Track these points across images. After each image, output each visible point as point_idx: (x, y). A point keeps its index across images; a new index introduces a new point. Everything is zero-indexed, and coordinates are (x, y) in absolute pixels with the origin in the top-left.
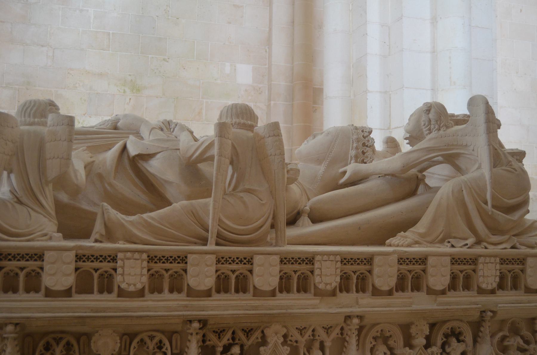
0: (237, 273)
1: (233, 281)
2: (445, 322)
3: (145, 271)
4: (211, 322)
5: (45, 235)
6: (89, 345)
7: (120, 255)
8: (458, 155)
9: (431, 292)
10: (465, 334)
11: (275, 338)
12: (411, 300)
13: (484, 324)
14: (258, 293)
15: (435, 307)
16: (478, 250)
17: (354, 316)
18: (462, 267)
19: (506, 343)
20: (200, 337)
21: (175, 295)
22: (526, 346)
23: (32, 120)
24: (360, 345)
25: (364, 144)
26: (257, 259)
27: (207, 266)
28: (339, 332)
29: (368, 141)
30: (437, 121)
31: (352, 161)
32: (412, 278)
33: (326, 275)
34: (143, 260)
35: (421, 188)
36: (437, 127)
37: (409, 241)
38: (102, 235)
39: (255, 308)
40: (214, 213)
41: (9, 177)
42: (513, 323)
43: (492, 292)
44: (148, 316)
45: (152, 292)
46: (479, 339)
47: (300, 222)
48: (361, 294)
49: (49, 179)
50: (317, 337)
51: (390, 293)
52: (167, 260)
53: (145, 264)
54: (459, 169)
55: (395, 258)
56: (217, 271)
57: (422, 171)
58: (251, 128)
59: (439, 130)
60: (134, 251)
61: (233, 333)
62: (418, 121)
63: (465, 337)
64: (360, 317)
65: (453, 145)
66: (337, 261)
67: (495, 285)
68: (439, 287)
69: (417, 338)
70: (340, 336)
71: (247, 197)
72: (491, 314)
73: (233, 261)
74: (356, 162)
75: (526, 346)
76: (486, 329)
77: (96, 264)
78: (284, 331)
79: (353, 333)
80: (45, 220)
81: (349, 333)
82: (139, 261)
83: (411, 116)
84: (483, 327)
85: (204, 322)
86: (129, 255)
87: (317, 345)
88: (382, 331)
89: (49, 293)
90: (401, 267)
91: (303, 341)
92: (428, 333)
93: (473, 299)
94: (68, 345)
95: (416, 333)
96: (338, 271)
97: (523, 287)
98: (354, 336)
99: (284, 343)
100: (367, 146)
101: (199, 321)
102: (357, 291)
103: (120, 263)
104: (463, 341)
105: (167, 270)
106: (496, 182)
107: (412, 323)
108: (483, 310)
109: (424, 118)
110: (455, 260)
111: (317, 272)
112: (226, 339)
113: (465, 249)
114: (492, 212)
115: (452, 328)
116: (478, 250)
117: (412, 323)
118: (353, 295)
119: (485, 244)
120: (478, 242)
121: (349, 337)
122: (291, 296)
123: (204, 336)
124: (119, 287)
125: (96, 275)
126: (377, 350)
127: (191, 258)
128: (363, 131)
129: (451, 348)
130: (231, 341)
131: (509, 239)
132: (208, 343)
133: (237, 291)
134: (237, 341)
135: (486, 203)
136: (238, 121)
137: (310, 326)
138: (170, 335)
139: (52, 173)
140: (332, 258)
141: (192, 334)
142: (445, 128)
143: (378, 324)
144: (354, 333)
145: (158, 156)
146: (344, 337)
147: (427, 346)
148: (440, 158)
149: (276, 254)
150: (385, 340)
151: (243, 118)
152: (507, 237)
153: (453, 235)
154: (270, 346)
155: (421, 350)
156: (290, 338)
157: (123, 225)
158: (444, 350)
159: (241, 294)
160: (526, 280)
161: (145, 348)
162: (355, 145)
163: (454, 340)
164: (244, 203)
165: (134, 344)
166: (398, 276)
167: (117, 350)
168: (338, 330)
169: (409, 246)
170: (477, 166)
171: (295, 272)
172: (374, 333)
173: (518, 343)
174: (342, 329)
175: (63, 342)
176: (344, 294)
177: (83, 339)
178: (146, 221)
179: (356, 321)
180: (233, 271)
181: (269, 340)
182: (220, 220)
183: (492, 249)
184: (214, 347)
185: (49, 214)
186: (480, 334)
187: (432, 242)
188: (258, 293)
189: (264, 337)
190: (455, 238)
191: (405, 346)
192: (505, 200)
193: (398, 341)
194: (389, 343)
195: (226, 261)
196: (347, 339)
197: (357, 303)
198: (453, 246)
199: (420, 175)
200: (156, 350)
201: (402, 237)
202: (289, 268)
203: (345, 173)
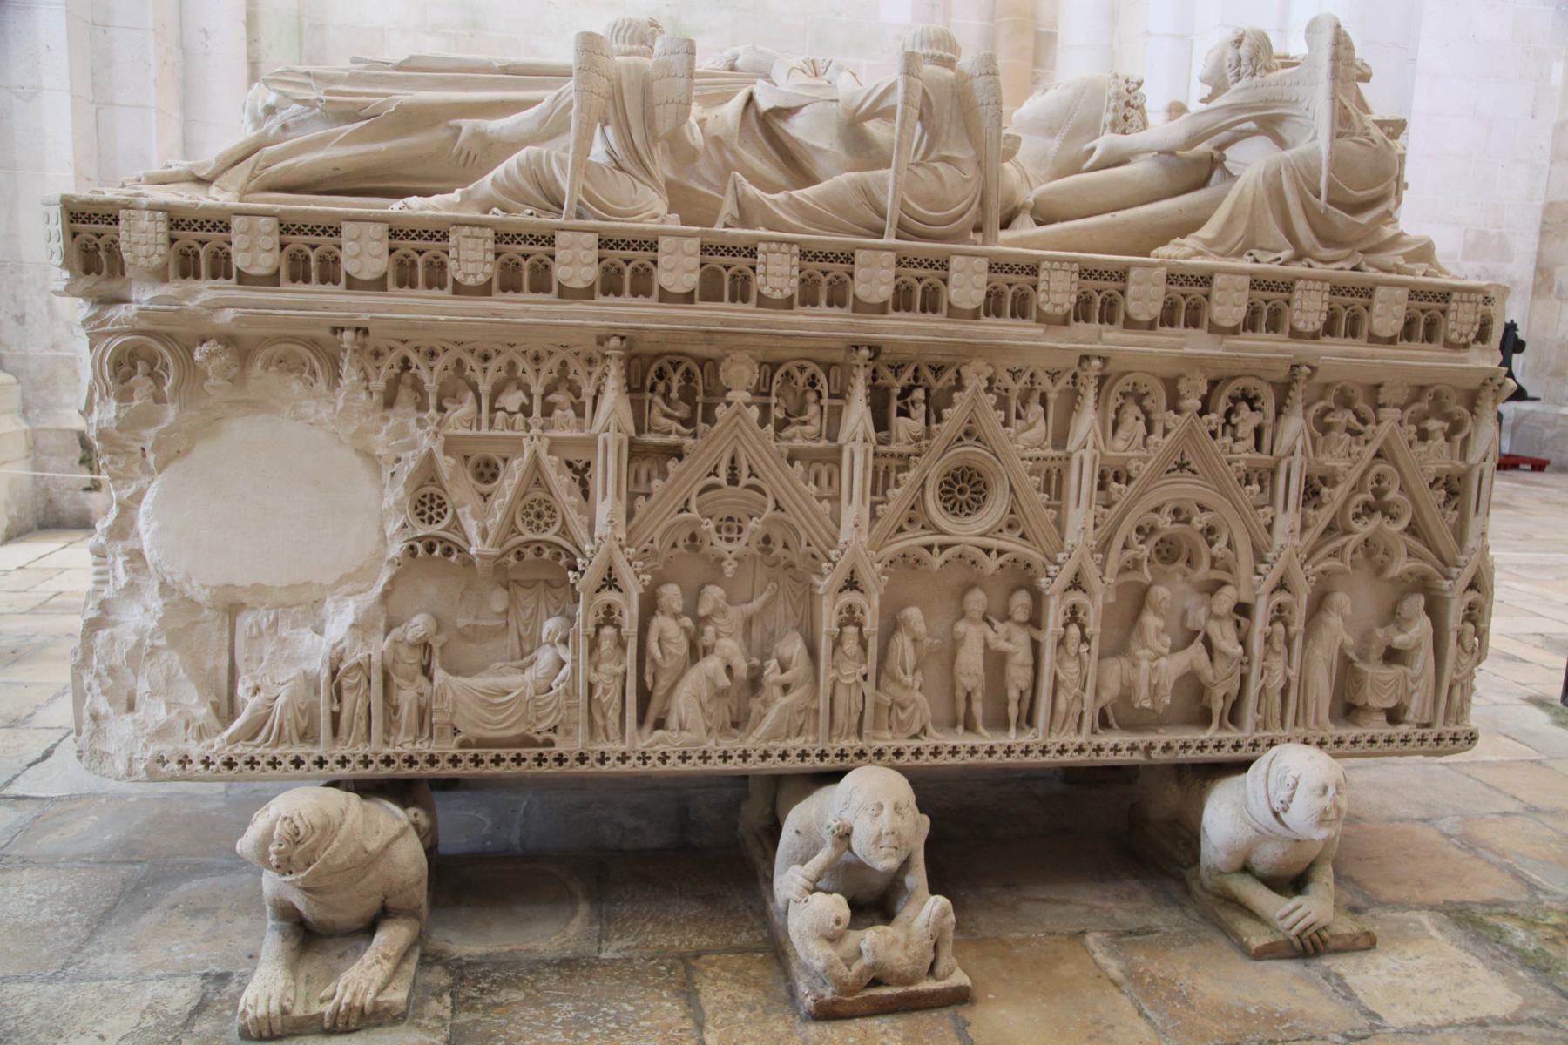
0: (924, 283)
1: (919, 294)
2: (1232, 378)
3: (795, 271)
4: (886, 350)
5: (656, 216)
6: (717, 376)
7: (761, 246)
8: (1279, 119)
9: (1215, 329)
11: (976, 381)
13: (1295, 386)
14: (954, 312)
15: (1219, 352)
16: (1297, 268)
17: (1094, 357)
18: (1268, 295)
19: (1328, 419)
20: (869, 371)
21: (836, 310)
22: (1360, 427)
23: (629, 47)
24: (1101, 403)
25: (1127, 104)
26: (955, 262)
27: (883, 267)
28: (1071, 380)
29: (1135, 98)
30: (1251, 60)
31: (1107, 131)
32: (1187, 308)
33: (1056, 292)
34: (793, 255)
35: (1217, 175)
36: (1250, 69)
37: (1187, 250)
38: (733, 218)
39: (950, 334)
40: (895, 190)
41: (603, 131)
42: (1343, 391)
43: (1314, 336)
44: (799, 335)
45: (803, 304)
46: (1285, 409)
47: (1014, 224)
48: (1106, 326)
49: (661, 134)
50: (1037, 386)
51: (1151, 326)
52: (826, 257)
53: (796, 260)
54: (1281, 143)
55: (1162, 272)
56: (896, 277)
57: (1222, 147)
58: (949, 63)
59: (1253, 74)
60: (780, 242)
61: (916, 370)
62: (1220, 60)
64: (1104, 360)
65: (1274, 100)
66: (1073, 272)
67: (1318, 326)
68: (1228, 323)
70: (1071, 385)
71: (942, 168)
72: (1309, 371)
73: (920, 264)
74: (1113, 131)
75: (1360, 427)
76: (1298, 395)
77: (727, 259)
78: (989, 371)
80: (654, 195)
81: (1085, 381)
82: (788, 257)
83: (1209, 52)
85: (876, 350)
86: (774, 246)
87: (1036, 396)
88: (1135, 384)
89: (665, 297)
90: (1171, 287)
91: (1016, 388)
92: (1205, 392)
93: (1281, 345)
94: (688, 374)
96: (1075, 287)
97: (1365, 332)
98: (1092, 386)
99: (989, 390)
100: (1133, 107)
101: (870, 348)
103: (761, 257)
104: (1260, 410)
105: (825, 273)
106: (1337, 162)
107: (1181, 376)
108: (1296, 363)
109: (1230, 55)
110: (1257, 283)
111: (1042, 286)
112: (906, 377)
113: (1275, 266)
114: (1327, 210)
115: (1244, 390)
116: (1297, 268)
117: (1181, 376)
118: (1095, 326)
119: (1309, 260)
120: (1298, 258)
122: (1001, 321)
123: (874, 371)
124: (759, 293)
125: (727, 275)
127: (860, 256)
128: (1127, 81)
130: (912, 382)
131: (1351, 255)
132: (880, 381)
133: (923, 310)
134: (920, 383)
135: (1318, 195)
136: (931, 52)
137: (1028, 368)
138: (828, 367)
139: (664, 127)
140: (1066, 266)
141: (858, 366)
142: (1264, 71)
143: (1129, 372)
145: (804, 110)
147: (1203, 412)
148: (1251, 125)
149: (983, 255)
150: (1139, 399)
151: (938, 48)
152: (1347, 251)
153: (1259, 244)
154: (968, 391)
156: (997, 384)
157: (764, 205)
158: (1228, 422)
159: (929, 315)
160: (1371, 321)
161: (792, 384)
162: (1112, 104)
163: (1244, 406)
164: (939, 177)
165: (777, 377)
166: (1165, 303)
167: (754, 383)
168: (1068, 377)
169: (1185, 258)
170: (1310, 136)
171: (1010, 285)
172: (1121, 386)
173: (1348, 420)
174: (1075, 376)
175: (682, 369)
176: (1081, 324)
177: (708, 365)
178: (796, 200)
179: (1096, 363)
180: (920, 280)
181: (966, 383)
182: (903, 202)
183: (1319, 269)
184: (887, 389)
185: (659, 186)
186: (1288, 401)
187: (1223, 255)
188: (954, 312)
189: (959, 379)
190: (1261, 249)
191: (1169, 408)
192: (1351, 191)
193: (1157, 400)
195: (910, 263)
197: (1100, 337)
198: (1256, 261)
199: (1216, 154)
200: (807, 387)
201: (1176, 244)
202: (1001, 279)
203: (1092, 150)
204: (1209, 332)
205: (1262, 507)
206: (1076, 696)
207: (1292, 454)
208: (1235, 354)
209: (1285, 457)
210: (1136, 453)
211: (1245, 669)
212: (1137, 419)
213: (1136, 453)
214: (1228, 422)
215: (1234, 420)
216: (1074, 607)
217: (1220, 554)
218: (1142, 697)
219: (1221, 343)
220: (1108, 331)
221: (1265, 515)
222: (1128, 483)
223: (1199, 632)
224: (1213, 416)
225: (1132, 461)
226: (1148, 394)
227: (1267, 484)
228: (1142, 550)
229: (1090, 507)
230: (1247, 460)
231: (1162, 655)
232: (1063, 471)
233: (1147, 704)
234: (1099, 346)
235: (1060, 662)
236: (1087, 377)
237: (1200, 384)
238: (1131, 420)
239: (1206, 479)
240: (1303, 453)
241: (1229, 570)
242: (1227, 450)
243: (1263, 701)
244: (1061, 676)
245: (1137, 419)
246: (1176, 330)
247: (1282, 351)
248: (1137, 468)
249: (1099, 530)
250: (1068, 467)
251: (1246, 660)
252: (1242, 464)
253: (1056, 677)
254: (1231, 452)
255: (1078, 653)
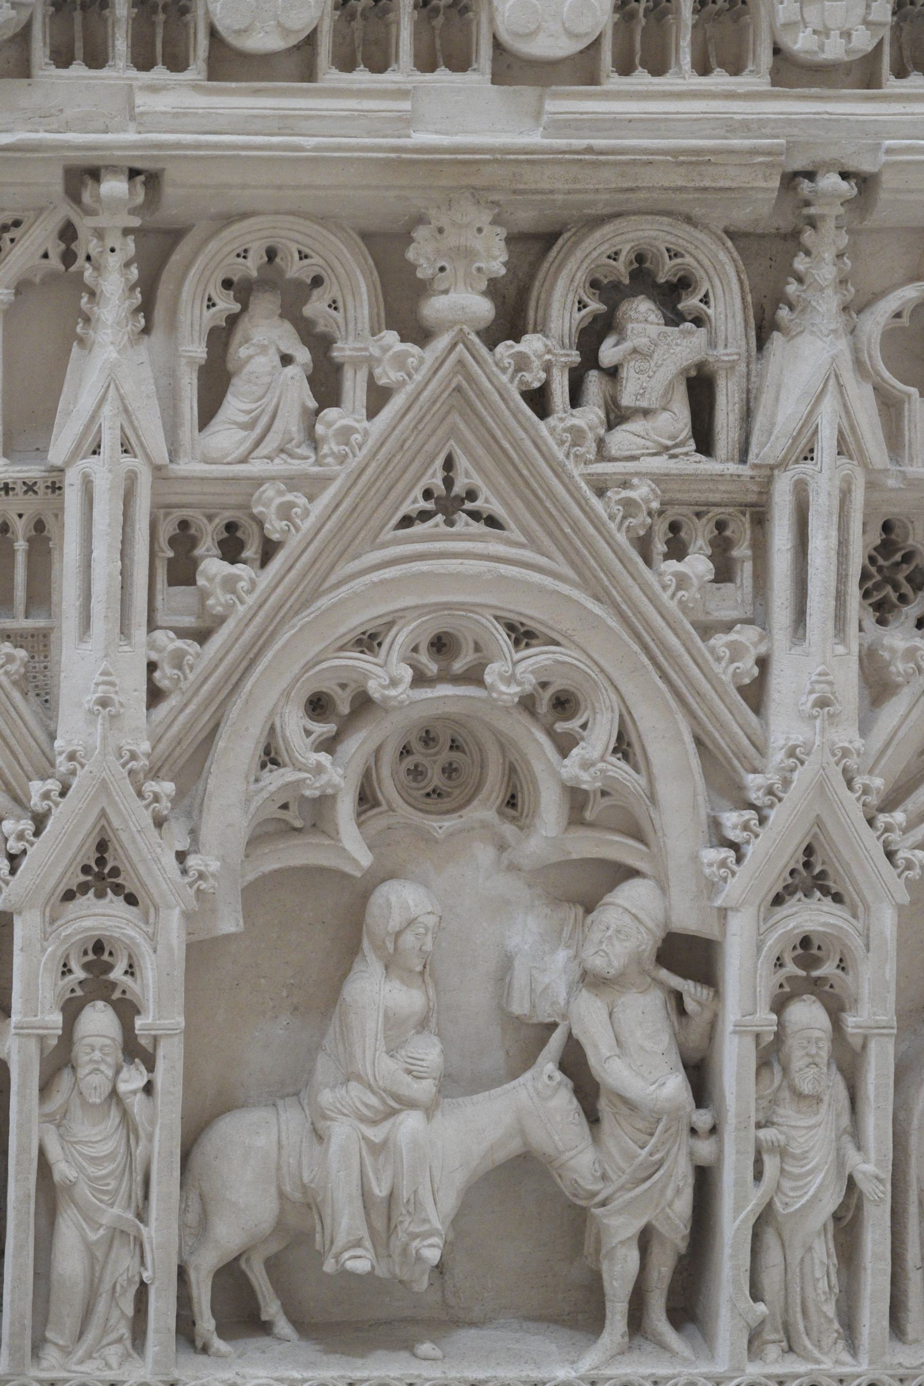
2: (600, 221)
10: (705, 287)
12: (406, 105)
13: (808, 236)
17: (113, 169)
48: (159, 73)
63: (705, 300)
69: (446, 292)
72: (847, 188)
79: (113, 250)
81: (93, 247)
84: (808, 253)
95: (439, 265)
98: (113, 262)
102: (144, 62)
108: (799, 163)
117: (420, 220)
121: (97, 268)
126: (247, 340)
129: (627, 345)
144: (117, 247)
146: (73, 269)
155: (461, 346)
158: (590, 359)
176: (78, 70)
186: (792, 288)
194: (308, 310)
196: (88, 273)
204: (497, 78)
205: (728, 627)
206: (117, 1233)
207: (808, 455)
208: (580, 143)
209: (782, 464)
210: (279, 466)
211: (705, 1149)
212: (286, 360)
213: (279, 466)
214: (590, 359)
215: (608, 353)
216: (99, 947)
217: (588, 781)
218: (341, 1240)
219: (538, 113)
220: (153, 89)
221: (736, 652)
222: (266, 558)
223: (553, 1026)
224: (532, 344)
225: (268, 491)
226: (317, 281)
227: (742, 551)
228: (319, 769)
229: (125, 630)
230: (658, 479)
231: (411, 1104)
232: (50, 522)
233: (360, 1265)
234: (131, 136)
235: (59, 1120)
236: (99, 234)
237: (478, 244)
238: (266, 363)
239: (533, 543)
240: (842, 450)
241: (638, 835)
242: (589, 448)
243: (773, 1256)
244: (62, 1170)
245: (286, 360)
246: (388, 79)
247: (746, 127)
248: (285, 511)
249: (163, 709)
250: (59, 513)
251: (703, 1119)
252: (641, 492)
253: (44, 1167)
254: (602, 454)
255: (114, 1093)
